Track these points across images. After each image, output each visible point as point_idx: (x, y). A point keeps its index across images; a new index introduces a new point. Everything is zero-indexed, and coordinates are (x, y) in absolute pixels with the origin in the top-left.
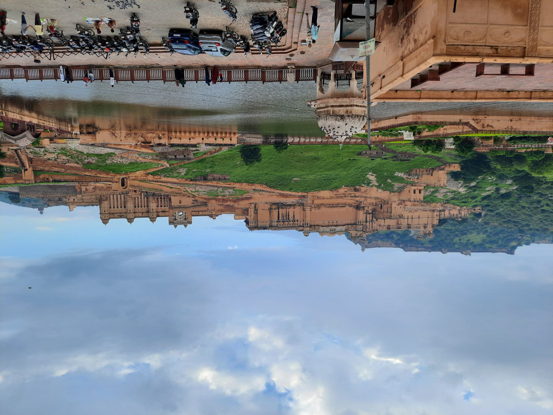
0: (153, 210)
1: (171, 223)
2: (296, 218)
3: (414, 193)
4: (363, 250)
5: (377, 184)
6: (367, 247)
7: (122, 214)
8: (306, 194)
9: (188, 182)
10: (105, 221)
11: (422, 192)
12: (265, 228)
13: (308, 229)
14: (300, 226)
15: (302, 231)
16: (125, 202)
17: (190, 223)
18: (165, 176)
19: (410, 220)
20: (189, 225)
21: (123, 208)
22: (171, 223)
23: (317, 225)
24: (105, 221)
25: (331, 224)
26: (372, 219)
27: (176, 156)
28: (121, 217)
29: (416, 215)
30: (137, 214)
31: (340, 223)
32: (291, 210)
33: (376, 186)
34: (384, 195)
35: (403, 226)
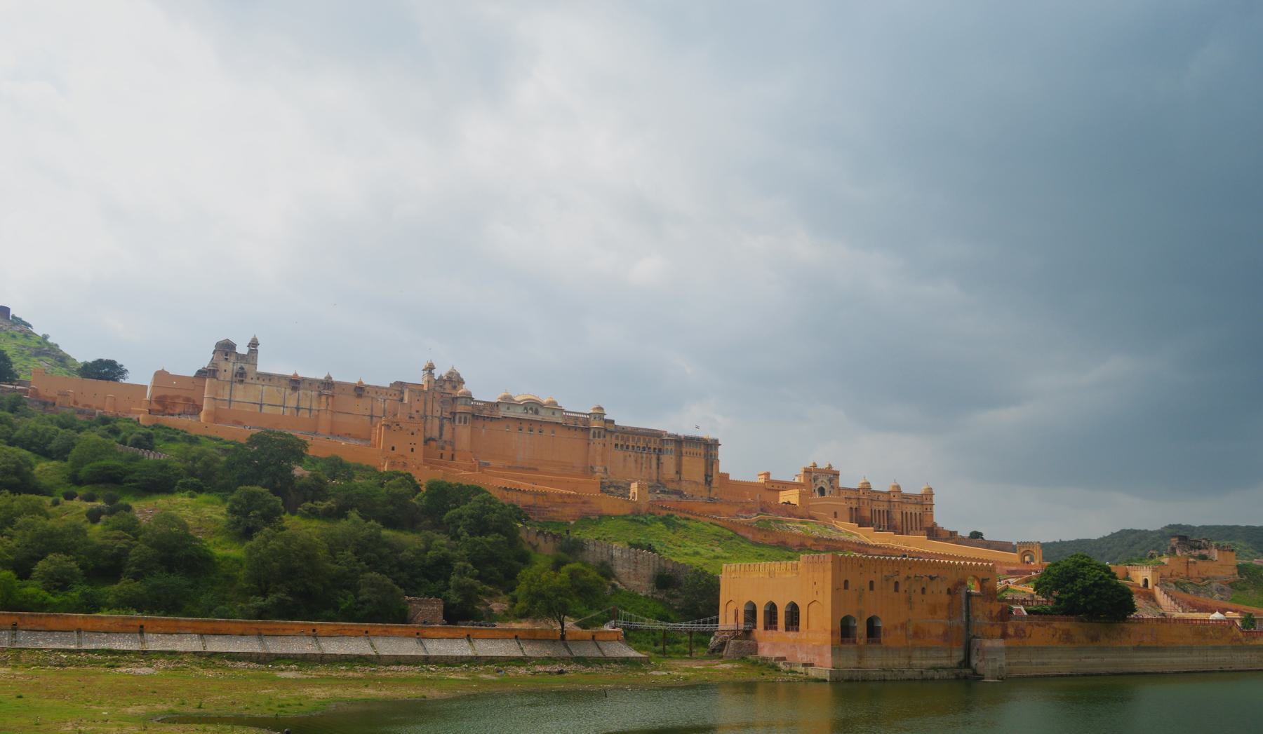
1: (837, 474)
15: (606, 421)
20: (809, 465)
22: (837, 474)
30: (885, 498)
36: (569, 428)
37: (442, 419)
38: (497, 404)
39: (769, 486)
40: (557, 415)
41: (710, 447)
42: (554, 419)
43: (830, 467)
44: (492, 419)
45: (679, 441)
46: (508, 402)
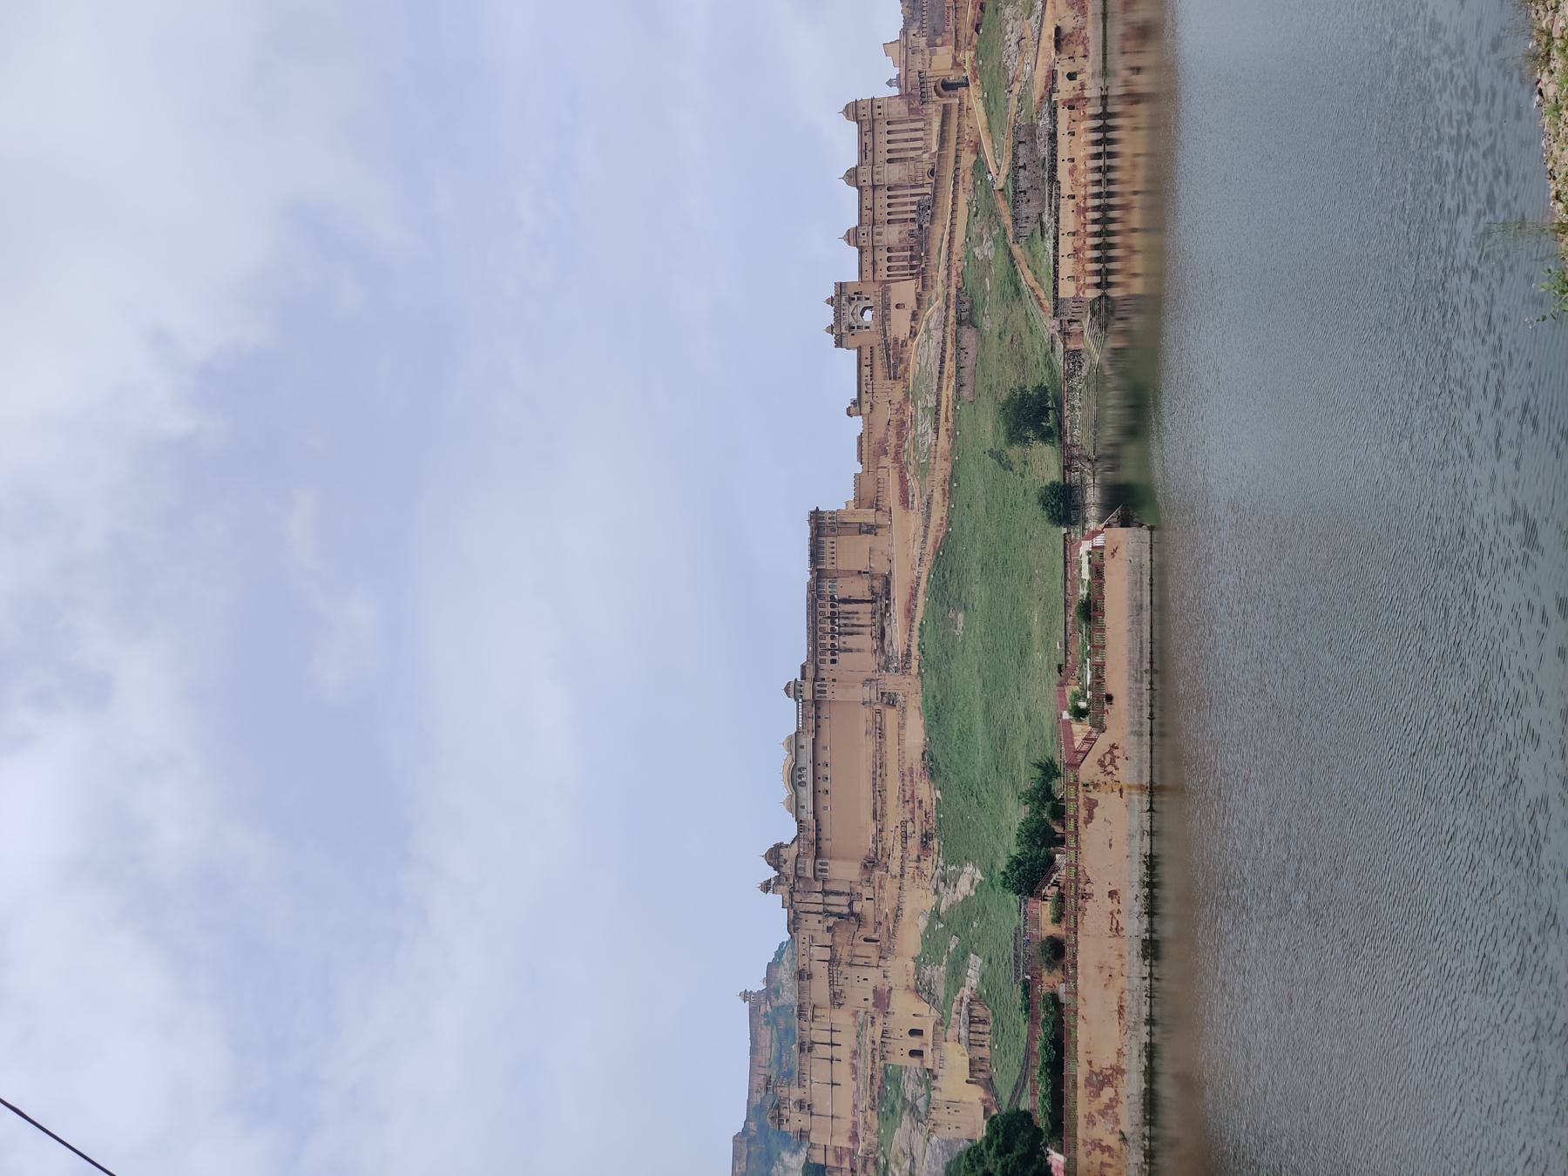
0: (880, 234)
1: (841, 287)
2: (841, 657)
3: (913, 1032)
4: (746, 996)
5: (943, 909)
6: (753, 1012)
7: (870, 155)
8: (914, 670)
9: (954, 279)
10: (853, 111)
11: (916, 1061)
12: (816, 555)
13: (808, 695)
14: (817, 669)
15: (803, 677)
16: (905, 159)
17: (839, 343)
18: (969, 204)
19: (826, 1051)
20: (832, 338)
21: (889, 156)
22: (841, 287)
23: (818, 726)
24: (853, 111)
25: (823, 771)
26: (832, 914)
27: (1024, 167)
28: (863, 152)
29: (843, 1072)
30: (868, 194)
31: (825, 801)
32: (866, 641)
33: (938, 906)
34: (910, 938)
35: (806, 1025)
36: (818, 726)
37: (826, 893)
38: (800, 822)
39: (866, 409)
40: (803, 742)
41: (821, 525)
42: (809, 747)
43: (831, 301)
44: (818, 830)
45: (819, 575)
46: (796, 807)
